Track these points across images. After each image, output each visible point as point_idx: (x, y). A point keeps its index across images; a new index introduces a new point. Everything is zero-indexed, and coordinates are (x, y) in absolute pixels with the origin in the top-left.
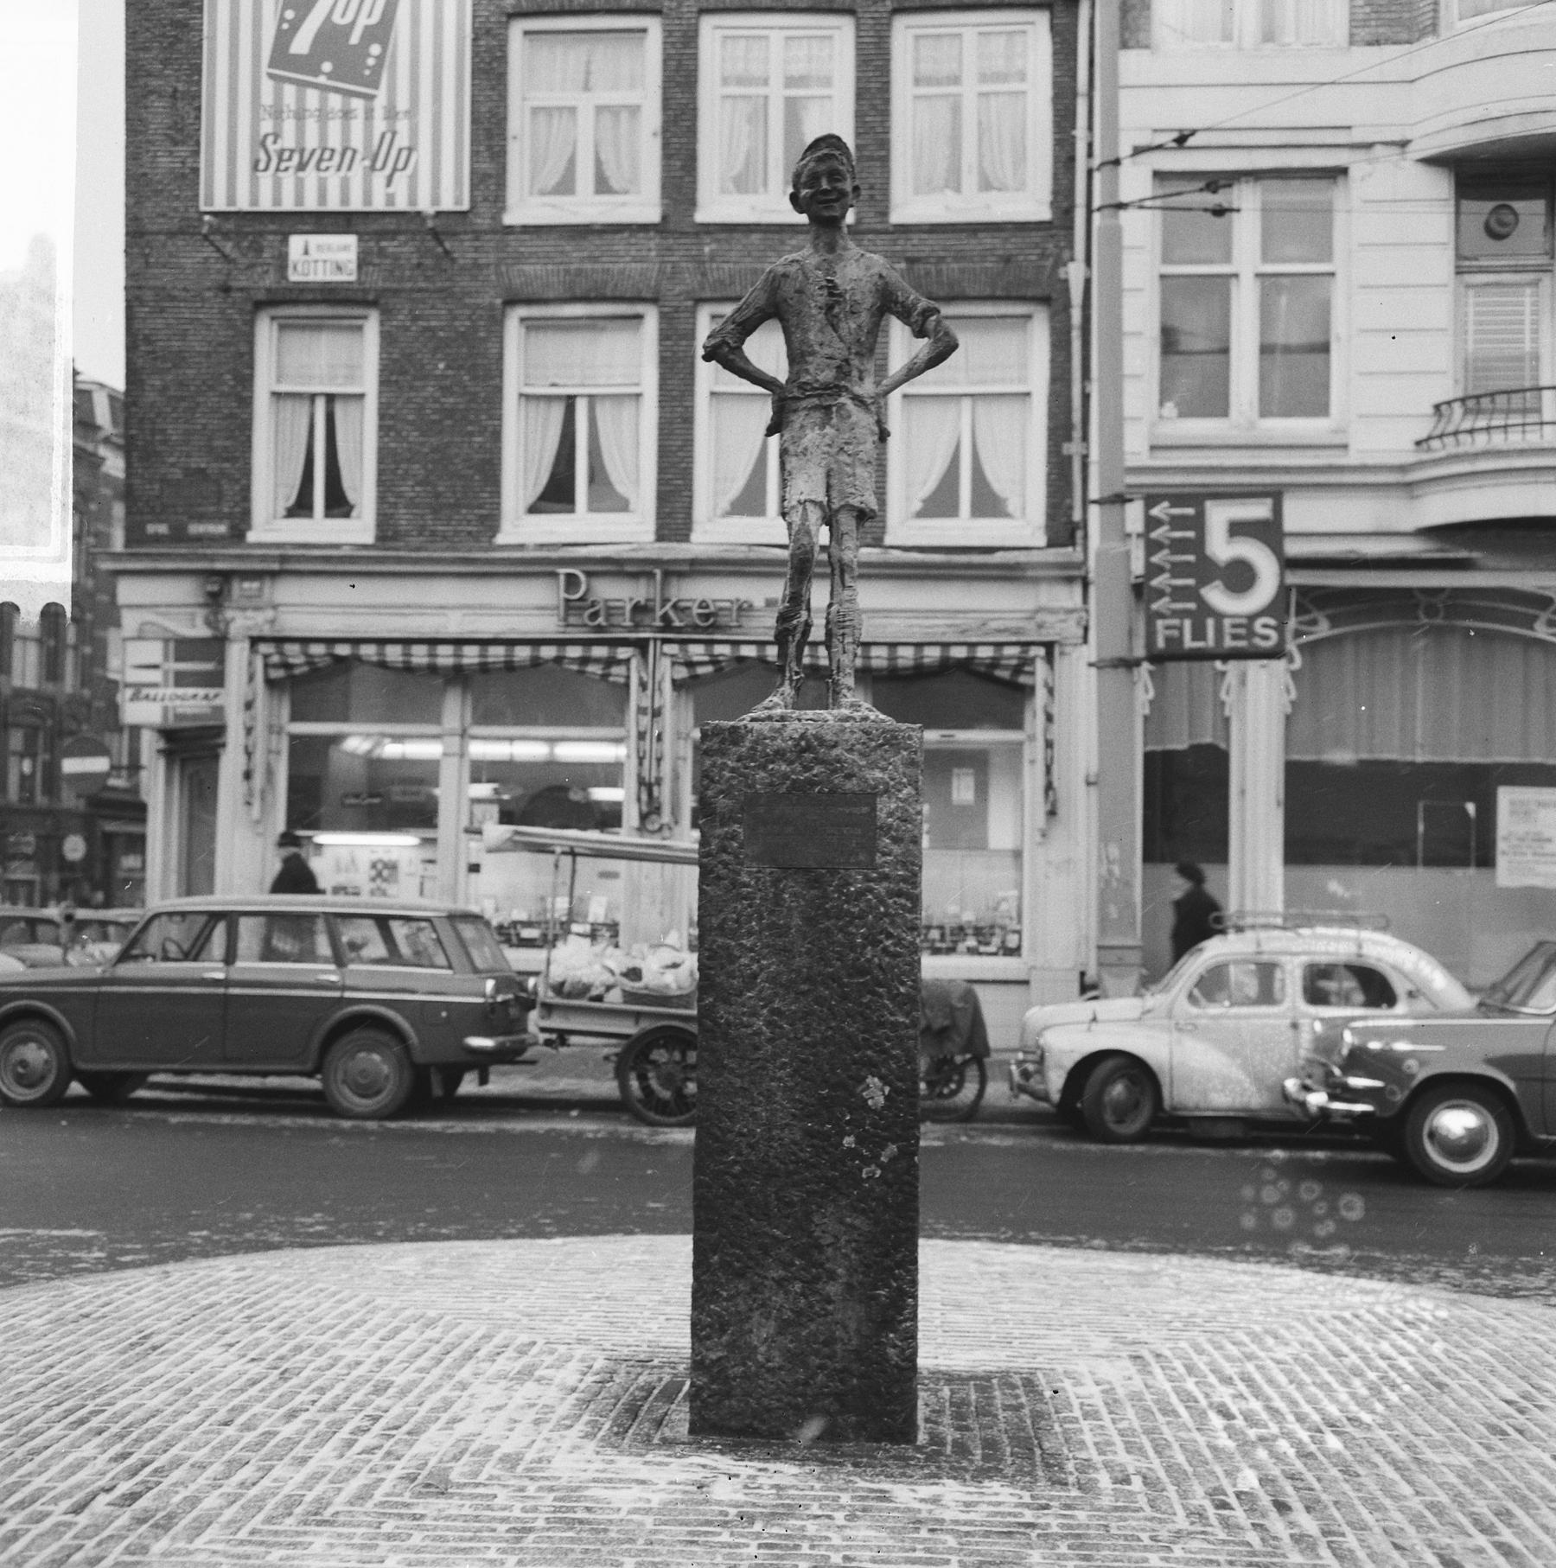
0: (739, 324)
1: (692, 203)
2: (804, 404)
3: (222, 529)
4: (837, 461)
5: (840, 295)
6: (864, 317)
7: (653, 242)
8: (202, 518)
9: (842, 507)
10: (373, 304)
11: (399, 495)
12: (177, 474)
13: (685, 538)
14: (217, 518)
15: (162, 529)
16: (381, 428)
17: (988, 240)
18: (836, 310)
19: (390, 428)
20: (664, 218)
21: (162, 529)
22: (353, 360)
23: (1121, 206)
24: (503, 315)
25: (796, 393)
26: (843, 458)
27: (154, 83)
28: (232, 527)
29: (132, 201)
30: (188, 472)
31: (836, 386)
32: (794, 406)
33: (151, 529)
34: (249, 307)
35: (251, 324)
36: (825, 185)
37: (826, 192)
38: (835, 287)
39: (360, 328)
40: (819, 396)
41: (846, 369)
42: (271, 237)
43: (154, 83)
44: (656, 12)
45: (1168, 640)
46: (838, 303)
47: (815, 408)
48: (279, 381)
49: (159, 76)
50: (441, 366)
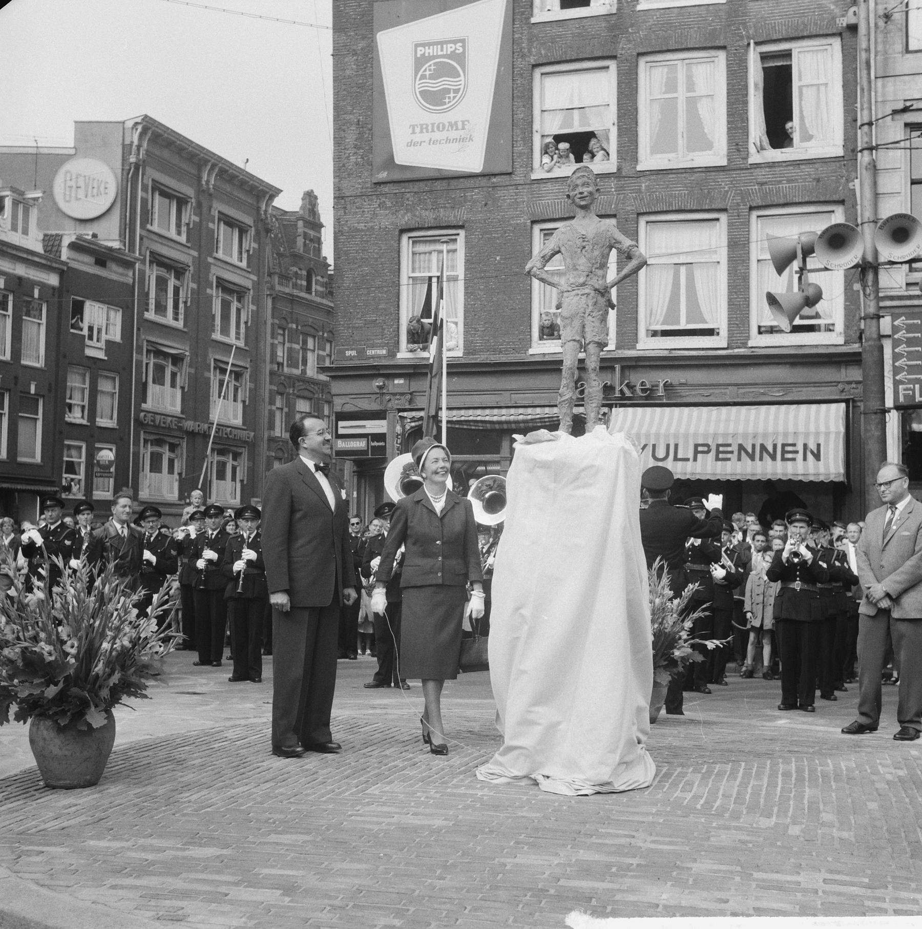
1: (635, 160)
3: (384, 352)
7: (612, 184)
8: (373, 347)
10: (462, 227)
11: (476, 330)
12: (360, 323)
13: (633, 347)
14: (381, 346)
15: (354, 353)
16: (466, 293)
17: (807, 169)
19: (472, 294)
20: (619, 169)
21: (354, 353)
22: (450, 260)
23: (876, 148)
24: (532, 228)
27: (348, 117)
28: (389, 351)
29: (337, 180)
30: (367, 323)
33: (348, 353)
34: (397, 233)
35: (399, 241)
39: (456, 240)
42: (408, 195)
43: (348, 117)
44: (614, 57)
45: (905, 396)
48: (413, 270)
49: (351, 113)
50: (498, 258)
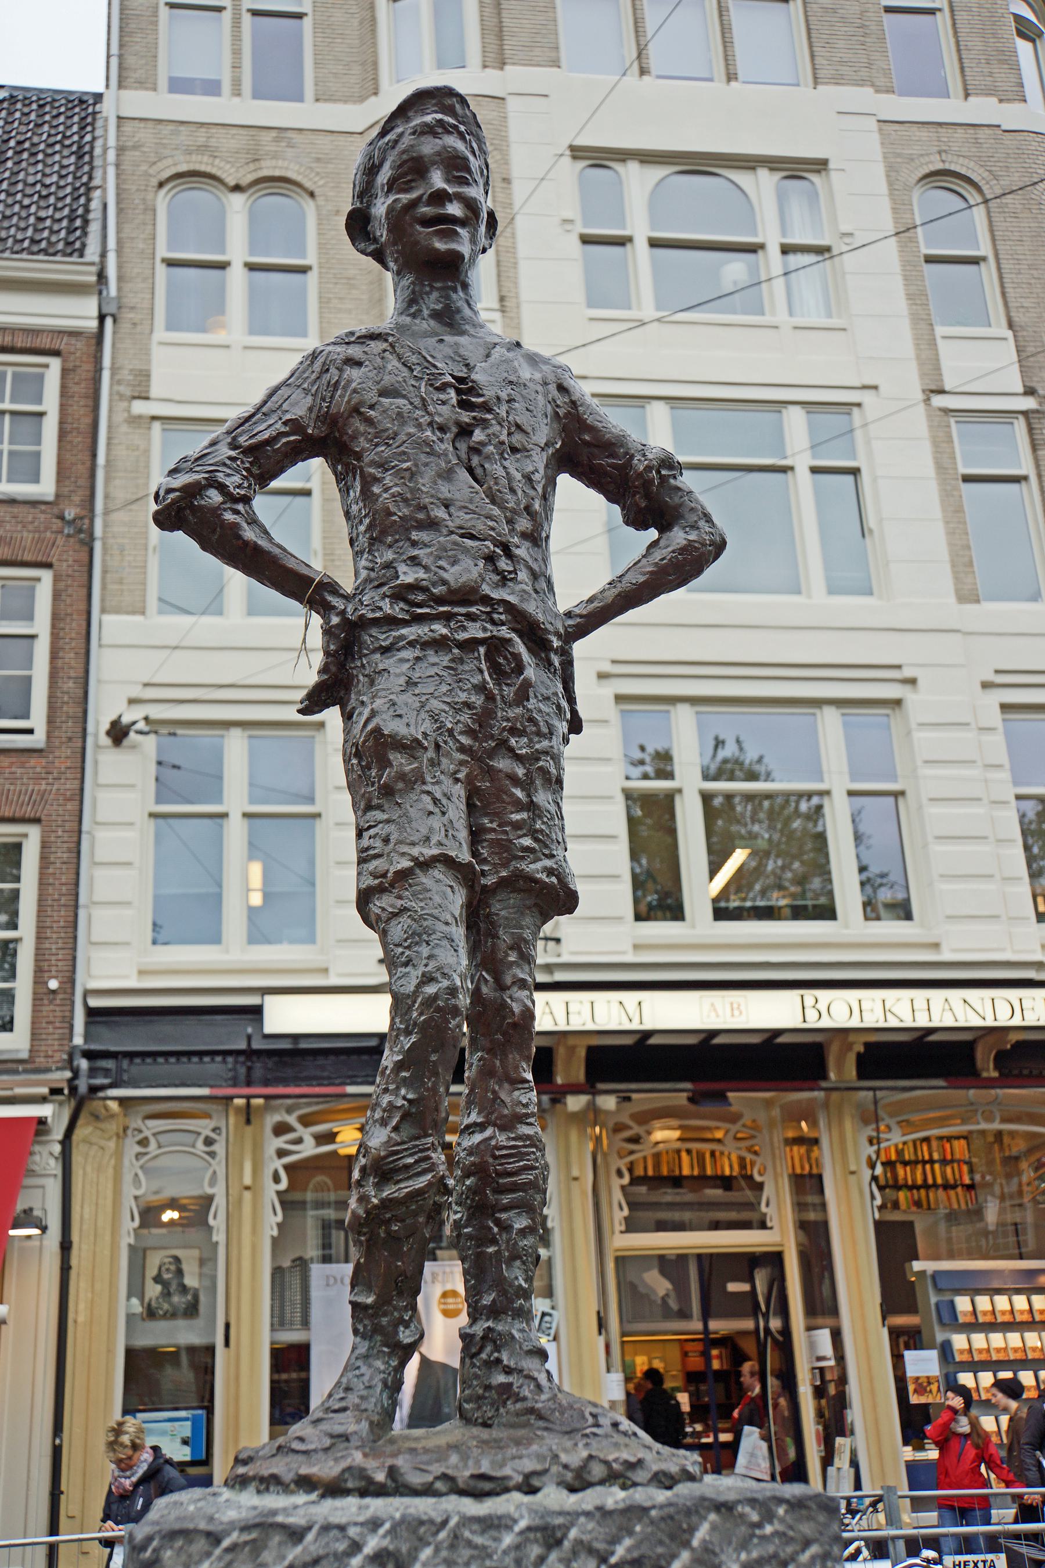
0: (249, 451)
2: (410, 632)
4: (491, 772)
5: (486, 407)
6: (539, 461)
9: (503, 883)
18: (478, 435)
25: (397, 610)
26: (503, 764)
31: (486, 600)
32: (384, 638)
36: (437, 180)
37: (440, 198)
38: (474, 390)
40: (447, 618)
41: (503, 564)
46: (484, 423)
47: (440, 644)
